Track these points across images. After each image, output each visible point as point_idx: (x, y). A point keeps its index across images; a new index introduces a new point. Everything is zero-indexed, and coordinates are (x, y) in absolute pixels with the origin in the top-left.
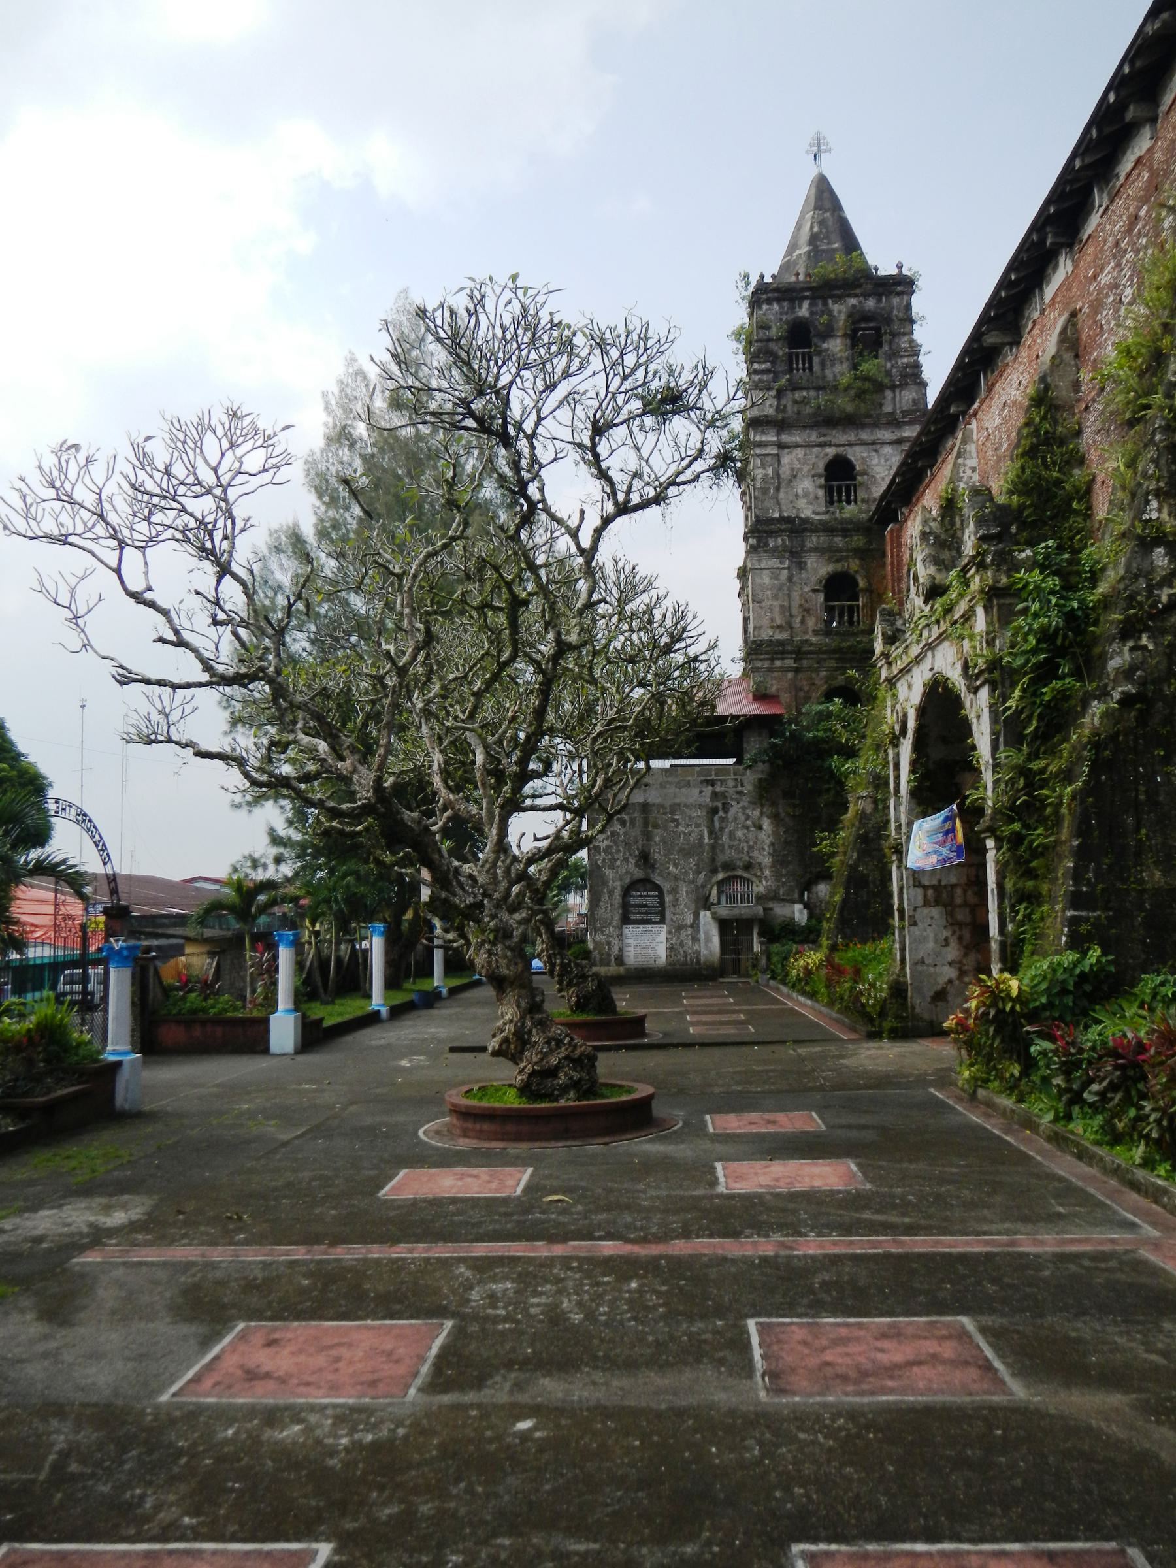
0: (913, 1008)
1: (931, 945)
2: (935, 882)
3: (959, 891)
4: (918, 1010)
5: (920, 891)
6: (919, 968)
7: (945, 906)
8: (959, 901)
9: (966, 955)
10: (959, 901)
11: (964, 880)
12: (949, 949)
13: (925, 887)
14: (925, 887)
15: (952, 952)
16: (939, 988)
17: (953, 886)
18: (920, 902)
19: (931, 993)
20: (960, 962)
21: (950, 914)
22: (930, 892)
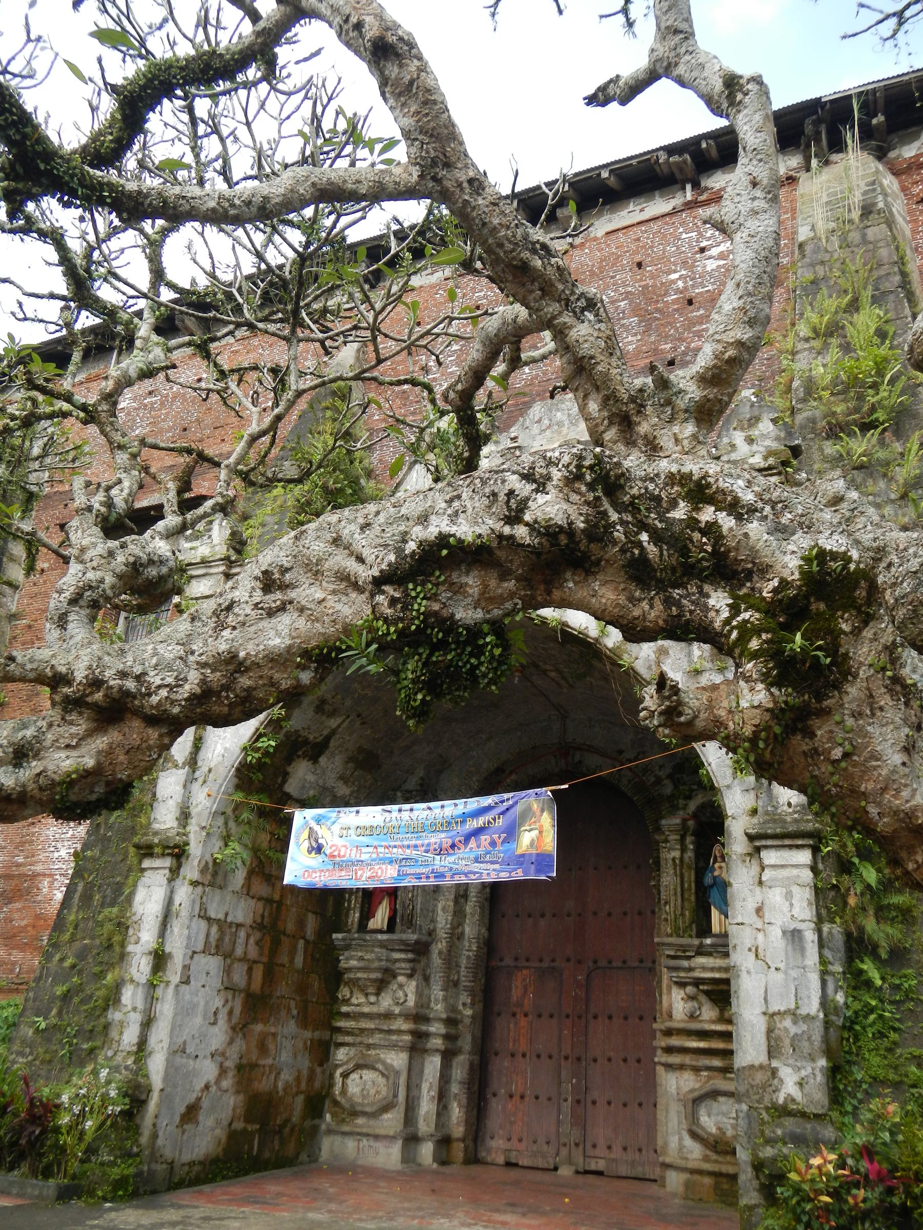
0: (155, 1136)
1: (198, 1020)
2: (221, 916)
3: (242, 934)
4: (160, 1142)
5: (203, 924)
6: (179, 1060)
7: (226, 956)
8: (239, 951)
9: (231, 1042)
10: (239, 951)
11: (249, 921)
12: (216, 1030)
13: (209, 919)
14: (209, 919)
15: (218, 1036)
16: (192, 1098)
17: (239, 926)
18: (200, 946)
19: (183, 1109)
20: (223, 1054)
21: (228, 971)
22: (214, 929)
